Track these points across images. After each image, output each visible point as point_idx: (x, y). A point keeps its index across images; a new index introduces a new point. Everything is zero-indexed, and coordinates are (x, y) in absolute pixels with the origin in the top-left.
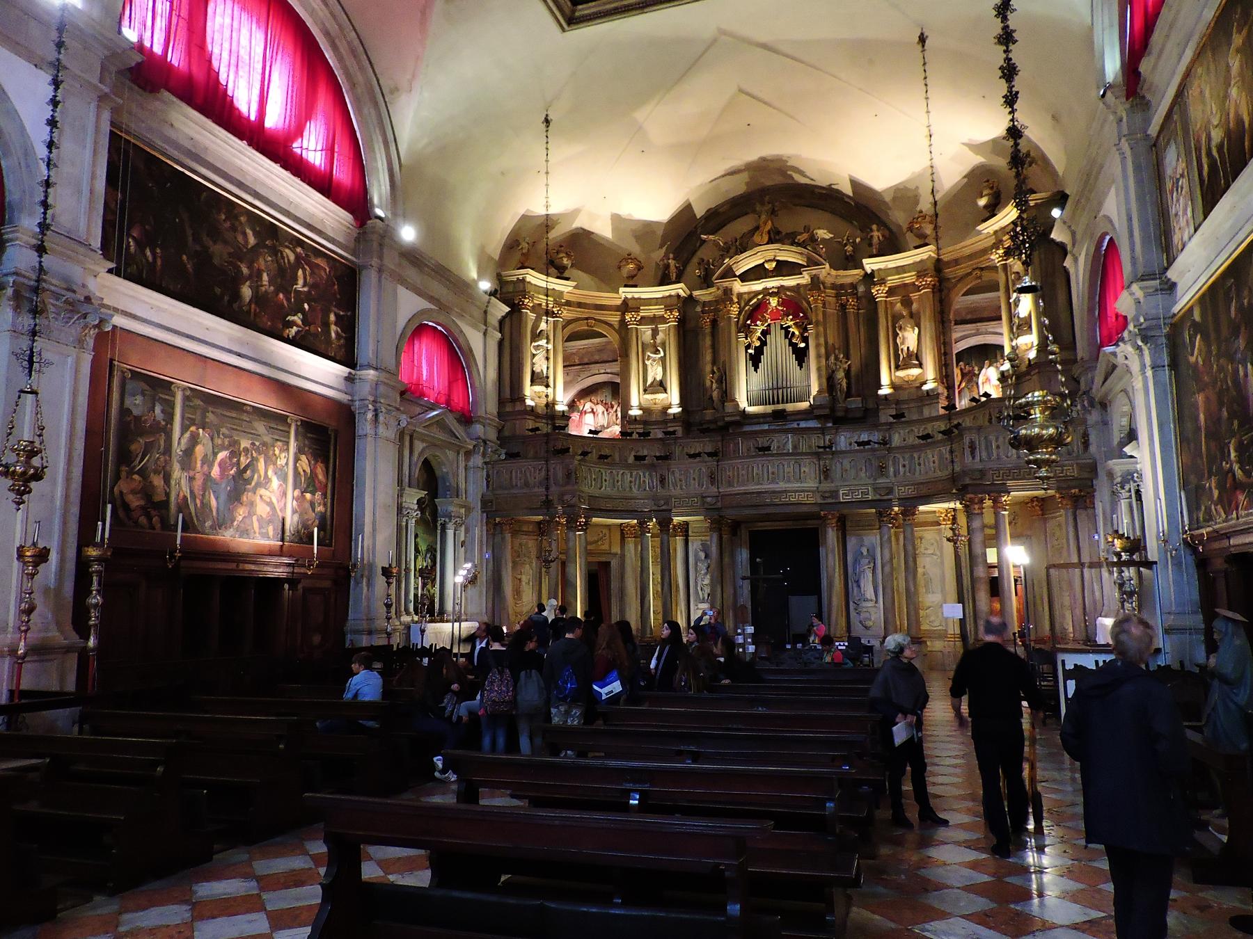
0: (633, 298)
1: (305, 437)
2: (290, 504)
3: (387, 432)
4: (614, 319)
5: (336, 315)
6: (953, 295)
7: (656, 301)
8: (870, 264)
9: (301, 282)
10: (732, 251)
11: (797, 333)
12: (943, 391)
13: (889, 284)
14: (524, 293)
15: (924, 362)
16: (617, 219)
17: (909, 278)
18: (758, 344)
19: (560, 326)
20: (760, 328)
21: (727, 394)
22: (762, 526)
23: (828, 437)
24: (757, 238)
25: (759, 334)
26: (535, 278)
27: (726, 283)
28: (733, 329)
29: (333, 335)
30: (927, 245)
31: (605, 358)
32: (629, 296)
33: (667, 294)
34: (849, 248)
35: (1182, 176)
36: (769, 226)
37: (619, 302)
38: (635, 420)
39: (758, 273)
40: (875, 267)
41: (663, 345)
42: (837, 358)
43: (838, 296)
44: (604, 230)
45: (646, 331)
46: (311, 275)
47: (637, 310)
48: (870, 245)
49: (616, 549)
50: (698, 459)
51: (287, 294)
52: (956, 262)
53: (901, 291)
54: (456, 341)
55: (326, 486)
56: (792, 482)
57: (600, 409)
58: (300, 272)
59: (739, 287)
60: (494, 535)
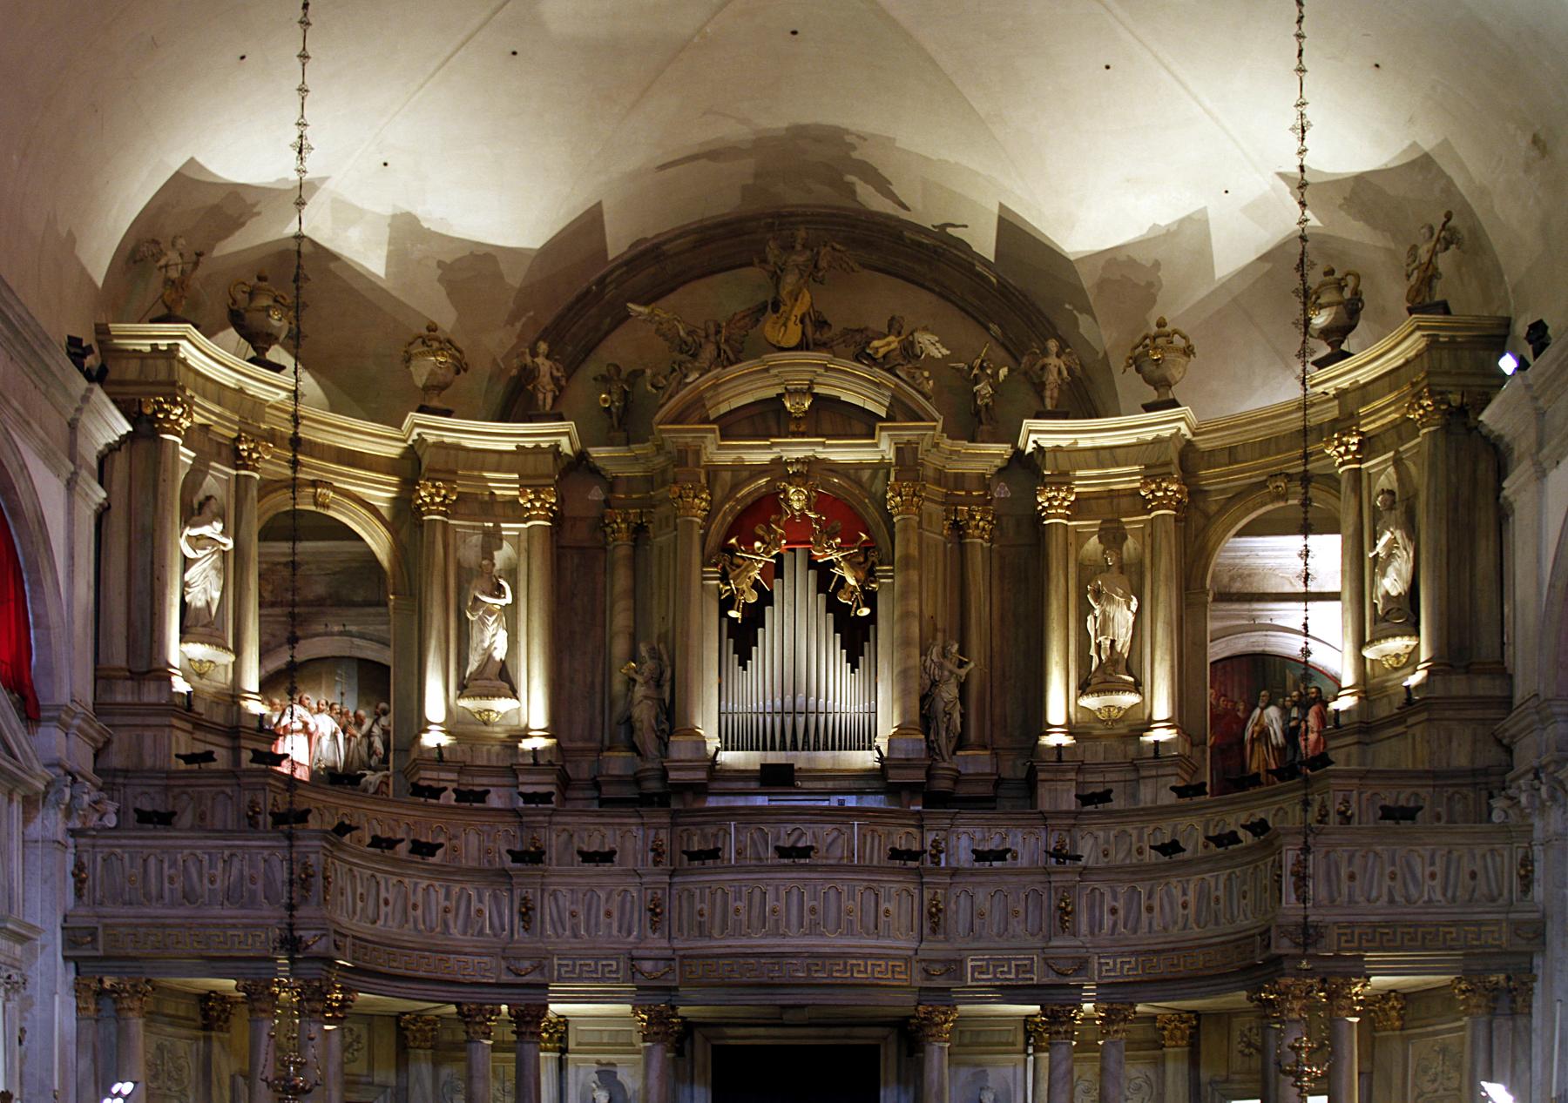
0: (441, 445)
7: (499, 460)
8: (1040, 434)
10: (709, 352)
16: (406, 232)
17: (1125, 478)
22: (737, 1037)
24: (770, 329)
27: (682, 435)
28: (697, 559)
30: (1174, 404)
33: (529, 443)
40: (1048, 442)
42: (944, 653)
44: (368, 255)
48: (1039, 388)
52: (1232, 454)
53: (1109, 510)
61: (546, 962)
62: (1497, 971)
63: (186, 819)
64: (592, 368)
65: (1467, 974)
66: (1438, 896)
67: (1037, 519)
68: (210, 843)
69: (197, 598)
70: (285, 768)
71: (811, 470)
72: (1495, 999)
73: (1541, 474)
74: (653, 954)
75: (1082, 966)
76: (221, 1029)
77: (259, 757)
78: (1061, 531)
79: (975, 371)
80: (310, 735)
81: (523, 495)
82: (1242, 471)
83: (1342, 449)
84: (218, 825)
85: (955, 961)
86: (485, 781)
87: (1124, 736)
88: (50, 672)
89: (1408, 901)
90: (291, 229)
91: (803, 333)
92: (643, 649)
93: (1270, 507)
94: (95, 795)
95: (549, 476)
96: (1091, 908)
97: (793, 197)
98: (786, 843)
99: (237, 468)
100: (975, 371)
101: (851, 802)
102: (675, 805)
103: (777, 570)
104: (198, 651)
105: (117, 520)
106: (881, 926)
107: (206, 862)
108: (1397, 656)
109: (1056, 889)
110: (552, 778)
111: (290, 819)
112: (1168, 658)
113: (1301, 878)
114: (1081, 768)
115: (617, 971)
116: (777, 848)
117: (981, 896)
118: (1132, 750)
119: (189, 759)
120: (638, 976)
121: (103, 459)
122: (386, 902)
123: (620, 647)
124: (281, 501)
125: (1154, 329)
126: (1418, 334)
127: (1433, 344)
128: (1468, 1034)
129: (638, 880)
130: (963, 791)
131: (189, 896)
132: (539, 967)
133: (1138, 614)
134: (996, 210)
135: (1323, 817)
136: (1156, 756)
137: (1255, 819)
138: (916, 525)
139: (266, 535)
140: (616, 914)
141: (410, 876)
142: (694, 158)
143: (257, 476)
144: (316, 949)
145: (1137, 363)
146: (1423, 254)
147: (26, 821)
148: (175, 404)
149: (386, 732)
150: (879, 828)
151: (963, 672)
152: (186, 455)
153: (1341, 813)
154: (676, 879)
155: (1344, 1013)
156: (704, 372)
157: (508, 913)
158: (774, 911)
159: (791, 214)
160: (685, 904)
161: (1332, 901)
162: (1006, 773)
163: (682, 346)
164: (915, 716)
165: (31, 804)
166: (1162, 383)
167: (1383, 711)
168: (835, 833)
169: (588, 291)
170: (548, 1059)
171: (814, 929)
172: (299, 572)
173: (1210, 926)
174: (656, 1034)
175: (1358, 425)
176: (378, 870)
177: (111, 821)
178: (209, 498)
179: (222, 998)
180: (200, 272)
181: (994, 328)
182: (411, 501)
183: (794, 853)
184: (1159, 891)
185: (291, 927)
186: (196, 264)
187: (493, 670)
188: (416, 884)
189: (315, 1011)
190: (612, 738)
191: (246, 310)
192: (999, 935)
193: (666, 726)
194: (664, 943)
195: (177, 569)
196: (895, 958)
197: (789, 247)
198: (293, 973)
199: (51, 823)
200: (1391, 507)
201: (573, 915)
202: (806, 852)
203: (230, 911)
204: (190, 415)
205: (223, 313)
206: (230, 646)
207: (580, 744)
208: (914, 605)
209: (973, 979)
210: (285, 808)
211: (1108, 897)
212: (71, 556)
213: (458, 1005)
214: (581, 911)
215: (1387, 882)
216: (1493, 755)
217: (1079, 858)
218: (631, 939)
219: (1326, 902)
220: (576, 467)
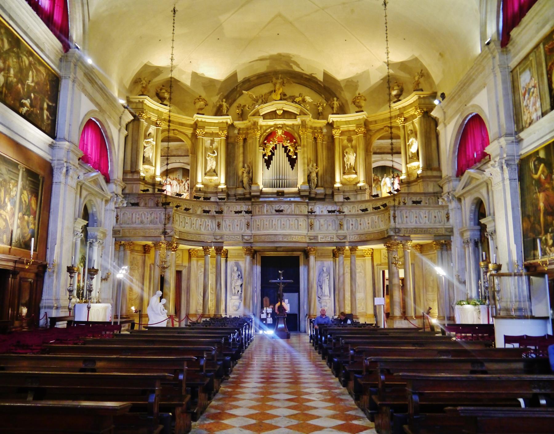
0: (201, 121)
1: (27, 179)
2: (17, 222)
3: (72, 182)
4: (189, 132)
5: (48, 105)
7: (214, 124)
8: (332, 118)
9: (30, 79)
10: (260, 101)
11: (292, 150)
12: (367, 187)
13: (342, 129)
14: (142, 111)
15: (358, 172)
16: (195, 76)
17: (352, 127)
18: (270, 154)
19: (160, 132)
20: (271, 145)
21: (252, 181)
23: (310, 207)
24: (274, 96)
25: (271, 149)
26: (150, 103)
27: (255, 119)
28: (258, 145)
29: (45, 117)
30: (362, 111)
31: (180, 153)
32: (199, 119)
33: (221, 121)
35: (534, 87)
36: (281, 91)
37: (192, 123)
38: (200, 190)
39: (273, 115)
40: (335, 120)
41: (217, 149)
42: (313, 166)
43: (313, 133)
44: (186, 80)
45: (207, 141)
46: (36, 76)
47: (203, 128)
48: (333, 108)
49: (186, 263)
50: (240, 214)
51: (23, 84)
52: (376, 122)
54: (105, 132)
55: (35, 213)
56: (287, 229)
57: (175, 183)
58: (31, 73)
59: (262, 122)
60: (119, 251)
62: (442, 240)
63: (142, 204)
64: (236, 104)
65: (435, 241)
66: (427, 221)
67: (332, 137)
69: (146, 155)
70: (165, 193)
72: (442, 246)
73: (445, 126)
75: (345, 237)
77: (159, 190)
84: (149, 206)
88: (112, 171)
89: (420, 223)
90: (170, 76)
92: (246, 165)
94: (122, 199)
96: (347, 224)
97: (279, 68)
98: (277, 209)
101: (292, 199)
102: (253, 200)
103: (275, 148)
104: (147, 166)
105: (130, 138)
110: (225, 194)
111: (166, 204)
114: (344, 192)
118: (355, 188)
119: (144, 191)
121: (127, 126)
123: (241, 165)
124: (166, 134)
125: (358, 95)
127: (420, 98)
128: (436, 255)
130: (318, 197)
131: (142, 222)
133: (356, 157)
135: (399, 203)
136: (360, 189)
138: (306, 138)
139: (162, 141)
142: (257, 60)
144: (170, 234)
145: (354, 102)
146: (417, 78)
147: (105, 206)
151: (317, 170)
152: (145, 124)
153: (404, 202)
156: (259, 105)
157: (215, 225)
161: (402, 223)
162: (327, 193)
163: (254, 100)
164: (306, 180)
165: (107, 201)
166: (360, 107)
167: (412, 179)
169: (234, 88)
170: (223, 260)
171: (284, 229)
177: (125, 205)
179: (149, 246)
181: (323, 96)
183: (279, 211)
184: (362, 220)
185: (165, 229)
186: (149, 83)
187: (212, 171)
194: (250, 232)
195: (143, 148)
197: (277, 79)
198: (165, 240)
199: (112, 206)
200: (412, 133)
201: (229, 226)
202: (282, 211)
205: (154, 93)
207: (231, 187)
208: (306, 156)
212: (119, 146)
214: (231, 224)
216: (437, 189)
220: (232, 126)
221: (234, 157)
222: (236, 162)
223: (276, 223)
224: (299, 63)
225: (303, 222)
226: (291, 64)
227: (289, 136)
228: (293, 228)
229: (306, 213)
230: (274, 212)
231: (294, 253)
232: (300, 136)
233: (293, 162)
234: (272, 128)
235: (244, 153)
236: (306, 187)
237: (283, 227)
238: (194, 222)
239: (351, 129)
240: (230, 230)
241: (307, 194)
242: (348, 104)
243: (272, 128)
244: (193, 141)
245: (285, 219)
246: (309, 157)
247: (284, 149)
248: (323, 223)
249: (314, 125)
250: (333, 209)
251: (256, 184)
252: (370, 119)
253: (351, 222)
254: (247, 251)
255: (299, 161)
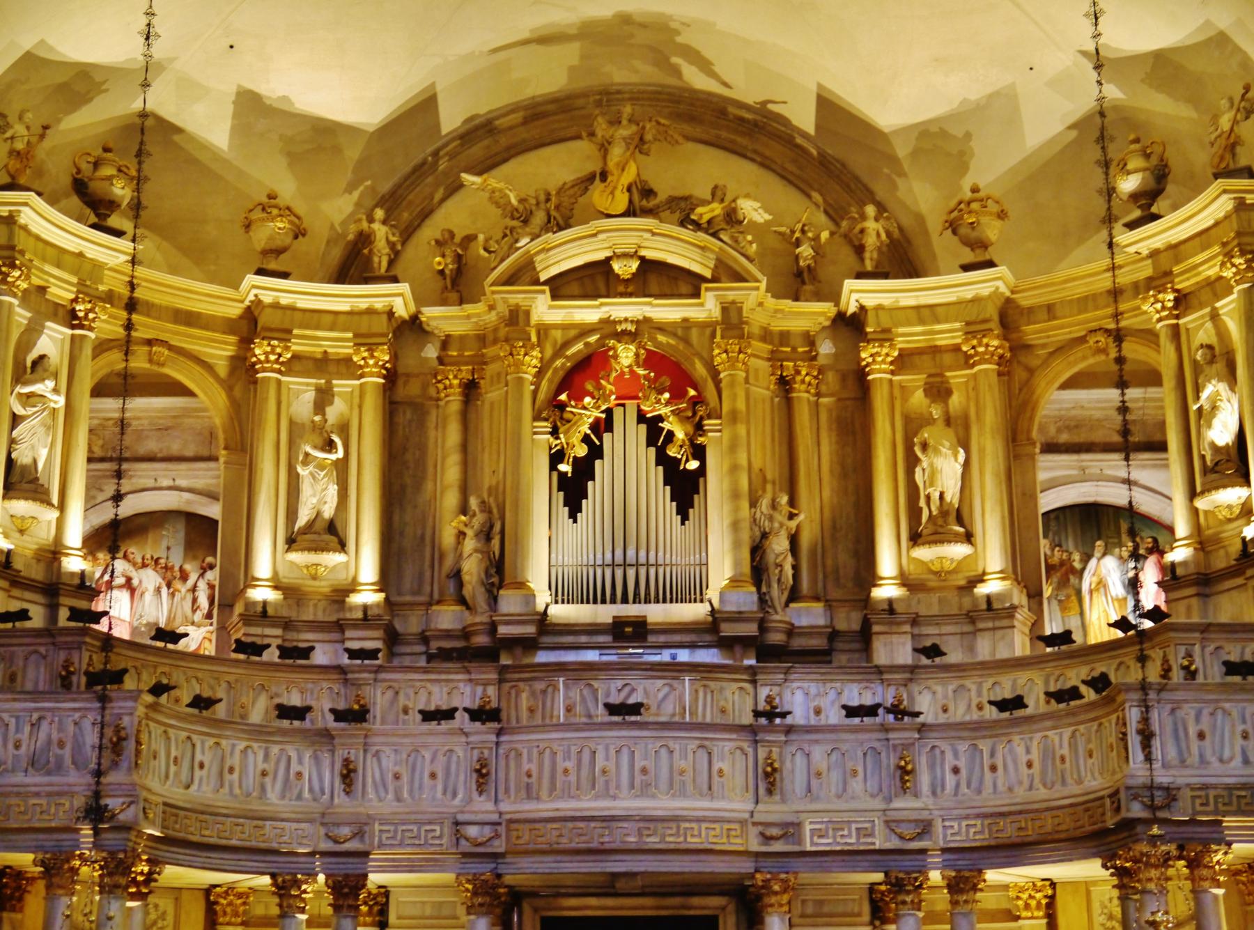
0: (276, 306)
4: (220, 351)
6: (1041, 383)
7: (334, 320)
8: (859, 294)
11: (680, 435)
12: (1019, 598)
13: (901, 342)
15: (978, 530)
16: (250, 106)
17: (948, 334)
18: (582, 451)
19: (88, 351)
20: (587, 414)
21: (501, 571)
23: (764, 692)
24: (597, 196)
25: (585, 429)
27: (516, 296)
30: (990, 264)
31: (175, 448)
32: (267, 298)
33: (363, 304)
34: (805, 251)
37: (235, 311)
38: (262, 614)
39: (594, 279)
40: (870, 301)
41: (344, 429)
42: (774, 505)
43: (775, 358)
44: (210, 126)
45: (301, 393)
47: (284, 334)
48: (860, 250)
50: (445, 725)
52: (1050, 310)
57: (149, 579)
59: (545, 310)
61: (366, 828)
64: (430, 232)
68: (18, 705)
69: (22, 456)
70: (103, 627)
71: (638, 331)
74: (480, 817)
75: (925, 828)
76: (13, 910)
77: (76, 614)
78: (886, 387)
79: (797, 235)
80: (132, 591)
81: (357, 352)
82: (1062, 327)
83: (1159, 306)
84: (29, 686)
85: (792, 824)
86: (310, 636)
87: (961, 588)
90: (137, 105)
91: (631, 201)
92: (473, 503)
93: (1091, 361)
95: (385, 335)
96: (932, 767)
98: (615, 699)
99: (73, 327)
100: (797, 235)
101: (684, 656)
102: (505, 660)
103: (604, 425)
106: (715, 787)
107: (12, 727)
108: (1230, 507)
109: (895, 746)
110: (379, 633)
112: (998, 509)
113: (1147, 737)
114: (915, 621)
115: (440, 837)
116: (607, 705)
117: (818, 753)
118: (967, 602)
120: (463, 842)
122: (202, 766)
123: (451, 499)
124: (114, 360)
125: (969, 195)
126: (1225, 197)
129: (463, 739)
130: (798, 643)
132: (359, 834)
133: (967, 465)
134: (814, 89)
135: (1166, 672)
137: (1096, 674)
138: (746, 381)
139: (98, 392)
140: (440, 775)
141: (227, 737)
143: (92, 335)
145: (953, 226)
146: (1225, 122)
148: (13, 266)
149: (211, 587)
150: (712, 684)
151: (793, 524)
152: (22, 316)
153: (1186, 668)
154: (503, 738)
155: (1206, 884)
157: (329, 776)
158: (604, 772)
159: (619, 92)
160: (512, 764)
161: (1183, 761)
162: (841, 625)
163: (513, 214)
164: (747, 569)
166: (984, 245)
167: (1221, 561)
168: (666, 689)
169: (424, 163)
171: (645, 790)
172: (129, 431)
173: (1058, 786)
174: (481, 905)
175: (1172, 282)
176: (194, 732)
178: (42, 357)
179: (18, 875)
180: (47, 144)
181: (817, 196)
182: (245, 359)
183: (624, 710)
185: (97, 795)
186: (42, 136)
187: (319, 526)
188: (234, 746)
189: (117, 886)
190: (441, 593)
191: (91, 180)
192: (839, 797)
193: (495, 580)
194: (490, 806)
196: (729, 822)
197: (616, 122)
198: (96, 846)
200: (1212, 360)
201: (397, 777)
202: (636, 709)
203: (35, 779)
204: (28, 277)
205: (66, 181)
206: (55, 501)
207: (408, 598)
208: (743, 459)
209: (812, 844)
210: (99, 669)
211: (949, 756)
213: (273, 876)
215: (1239, 742)
217: (917, 714)
218: (457, 801)
219: (1176, 762)
220: (412, 327)
221: (421, 463)
222: (429, 486)
223: (611, 766)
224: (708, 53)
225: (733, 761)
226: (675, 60)
227: (668, 371)
228: (689, 787)
229: (748, 719)
230: (601, 714)
231: (696, 901)
232: (715, 374)
233: (685, 488)
234: (593, 339)
235: (464, 447)
236: (746, 599)
237: (644, 783)
238: (236, 761)
239: (943, 341)
240: (399, 799)
241: (751, 629)
242: (926, 232)
243: (593, 339)
244: (238, 392)
245: (653, 746)
246: (757, 464)
247: (643, 428)
248: (823, 766)
249: (779, 325)
250: (868, 700)
251: (521, 585)
252: (1025, 300)
253: (950, 760)
254: (475, 893)
255: (715, 484)
